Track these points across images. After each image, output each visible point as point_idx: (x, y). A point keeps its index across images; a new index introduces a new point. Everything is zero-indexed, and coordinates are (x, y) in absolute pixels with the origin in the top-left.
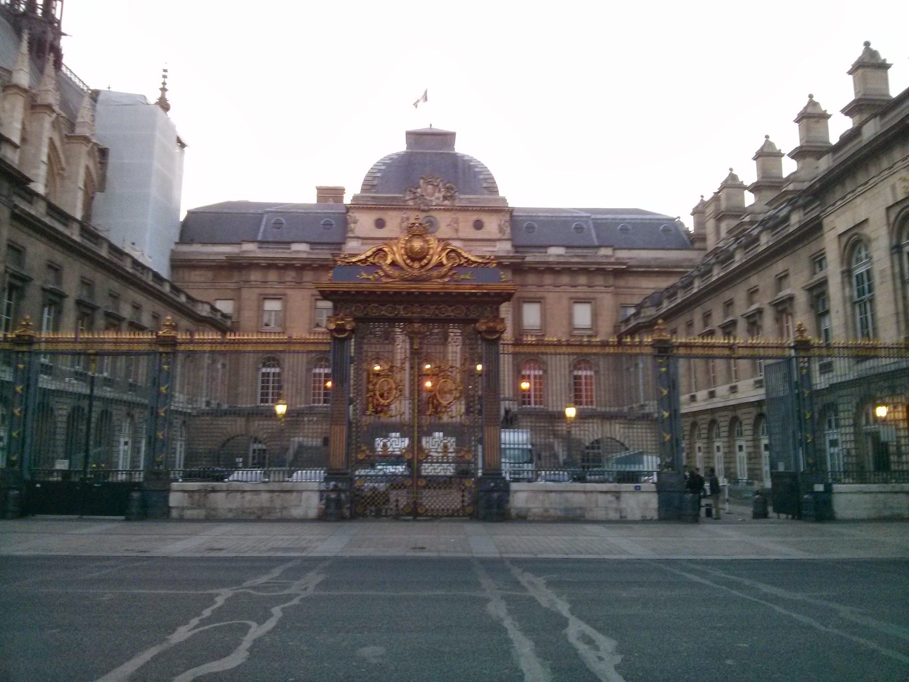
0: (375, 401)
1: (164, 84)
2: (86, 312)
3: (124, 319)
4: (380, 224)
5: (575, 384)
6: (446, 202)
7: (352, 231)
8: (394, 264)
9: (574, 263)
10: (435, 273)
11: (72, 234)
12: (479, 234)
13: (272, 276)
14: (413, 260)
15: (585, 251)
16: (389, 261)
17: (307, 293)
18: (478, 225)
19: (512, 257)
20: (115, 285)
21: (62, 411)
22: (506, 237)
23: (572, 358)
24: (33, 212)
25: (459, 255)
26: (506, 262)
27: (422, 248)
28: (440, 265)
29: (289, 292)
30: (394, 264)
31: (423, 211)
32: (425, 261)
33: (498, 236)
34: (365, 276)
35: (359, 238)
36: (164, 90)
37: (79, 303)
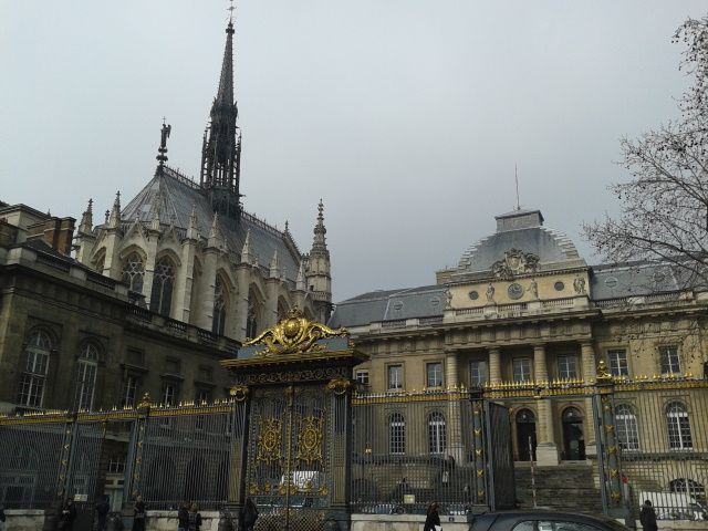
1: (320, 214)
4: (474, 295)
5: (670, 426)
6: (530, 270)
7: (449, 305)
9: (652, 310)
12: (561, 294)
13: (394, 348)
14: (289, 337)
15: (664, 298)
17: (420, 359)
18: (559, 286)
19: (586, 312)
21: (182, 463)
22: (581, 294)
23: (665, 400)
24: (151, 326)
25: (320, 330)
26: (582, 316)
27: (294, 328)
28: (308, 339)
29: (406, 359)
30: (277, 342)
33: (575, 294)
35: (454, 310)
36: (321, 218)
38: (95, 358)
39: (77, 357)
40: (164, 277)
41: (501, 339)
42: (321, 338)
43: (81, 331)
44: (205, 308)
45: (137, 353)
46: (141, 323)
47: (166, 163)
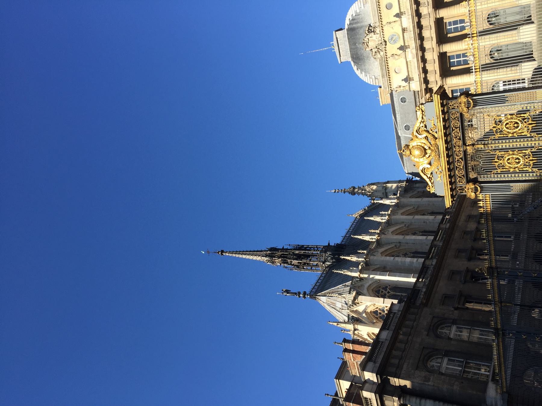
0: (522, 167)
2: (475, 254)
3: (477, 228)
8: (430, 164)
10: (433, 142)
11: (432, 265)
14: (426, 153)
16: (429, 166)
20: (457, 235)
24: (424, 290)
27: (418, 148)
28: (426, 138)
31: (386, 45)
32: (426, 147)
34: (439, 179)
37: (470, 259)
38: (451, 326)
39: (449, 339)
40: (389, 292)
41: (431, 43)
42: (426, 127)
43: (428, 335)
44: (412, 263)
45: (446, 298)
46: (422, 296)
47: (308, 292)
